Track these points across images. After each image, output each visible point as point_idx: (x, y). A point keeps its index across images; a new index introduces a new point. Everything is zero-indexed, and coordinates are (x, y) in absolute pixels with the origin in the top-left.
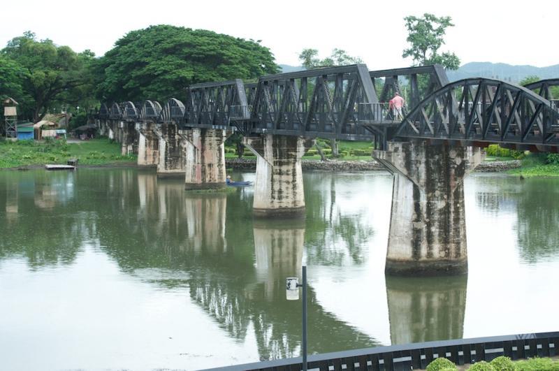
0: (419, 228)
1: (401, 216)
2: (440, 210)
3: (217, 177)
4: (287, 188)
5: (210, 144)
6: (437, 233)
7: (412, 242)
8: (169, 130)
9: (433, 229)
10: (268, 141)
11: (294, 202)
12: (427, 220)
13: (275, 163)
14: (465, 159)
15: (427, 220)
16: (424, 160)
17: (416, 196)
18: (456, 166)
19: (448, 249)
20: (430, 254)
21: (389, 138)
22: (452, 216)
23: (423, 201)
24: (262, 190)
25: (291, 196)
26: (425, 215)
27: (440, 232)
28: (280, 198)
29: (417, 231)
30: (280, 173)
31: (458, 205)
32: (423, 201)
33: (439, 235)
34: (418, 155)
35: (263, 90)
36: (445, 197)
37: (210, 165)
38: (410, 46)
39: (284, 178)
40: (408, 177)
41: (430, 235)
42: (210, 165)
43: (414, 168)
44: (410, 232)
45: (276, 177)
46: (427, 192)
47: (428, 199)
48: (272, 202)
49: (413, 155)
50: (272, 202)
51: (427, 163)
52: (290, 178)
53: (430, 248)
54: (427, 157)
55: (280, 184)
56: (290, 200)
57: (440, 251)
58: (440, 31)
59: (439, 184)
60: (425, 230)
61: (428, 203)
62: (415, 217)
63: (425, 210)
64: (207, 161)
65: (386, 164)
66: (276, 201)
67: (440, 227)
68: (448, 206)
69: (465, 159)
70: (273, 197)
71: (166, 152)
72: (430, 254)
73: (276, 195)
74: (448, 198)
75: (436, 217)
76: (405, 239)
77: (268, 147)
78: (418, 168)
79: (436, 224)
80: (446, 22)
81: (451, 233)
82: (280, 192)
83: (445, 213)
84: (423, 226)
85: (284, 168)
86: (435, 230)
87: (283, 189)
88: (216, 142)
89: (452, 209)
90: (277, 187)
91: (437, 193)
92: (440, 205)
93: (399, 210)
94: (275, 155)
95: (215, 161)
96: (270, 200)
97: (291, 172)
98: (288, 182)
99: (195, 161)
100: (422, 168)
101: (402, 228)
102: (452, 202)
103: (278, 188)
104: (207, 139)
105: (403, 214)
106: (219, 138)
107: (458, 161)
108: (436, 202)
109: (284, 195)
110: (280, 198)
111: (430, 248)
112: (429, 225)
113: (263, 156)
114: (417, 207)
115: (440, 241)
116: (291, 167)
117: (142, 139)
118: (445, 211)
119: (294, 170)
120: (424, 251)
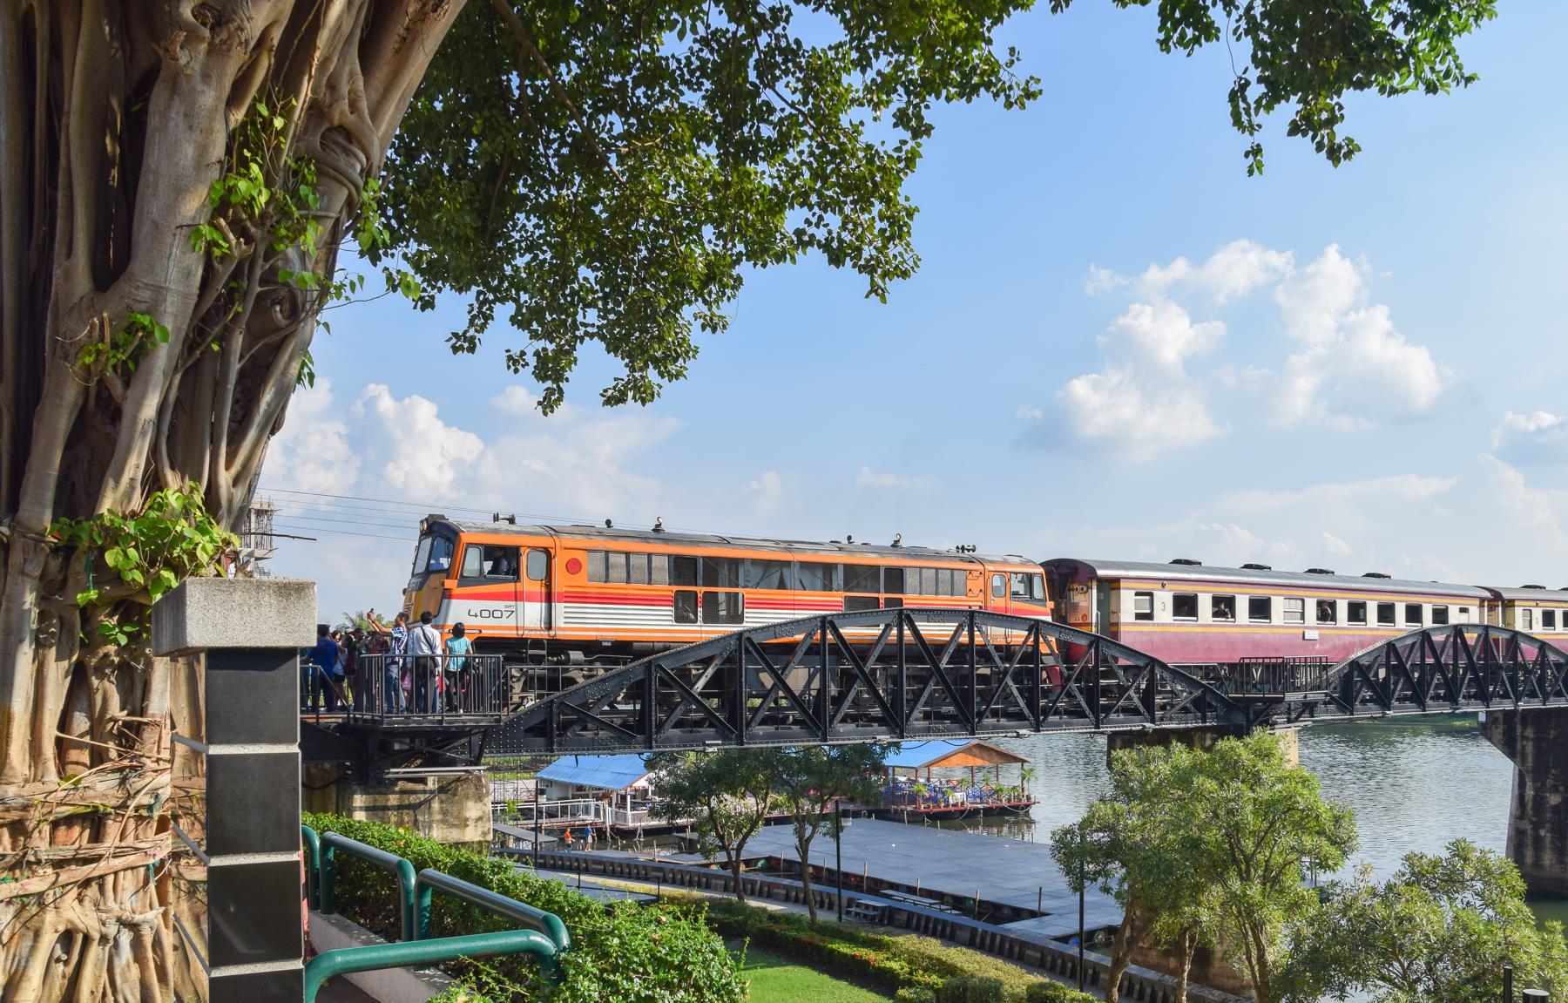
0: (1522, 828)
2: (1554, 807)
9: (1542, 833)
12: (1534, 819)
15: (1534, 819)
16: (1532, 736)
17: (1522, 785)
23: (1530, 793)
26: (1530, 812)
27: (1552, 838)
33: (1552, 842)
34: (1524, 728)
41: (1538, 841)
46: (1535, 781)
47: (1536, 790)
49: (1519, 730)
51: (1537, 741)
60: (1529, 832)
62: (1518, 812)
63: (1530, 804)
67: (1553, 831)
78: (1523, 747)
84: (1529, 827)
91: (1549, 782)
92: (1554, 800)
100: (1529, 748)
112: (1537, 826)
115: (1552, 850)
120: (1529, 859)
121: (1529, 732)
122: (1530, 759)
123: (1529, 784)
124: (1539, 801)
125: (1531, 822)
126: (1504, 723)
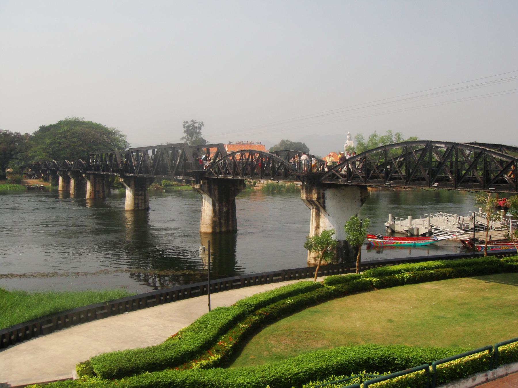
1: (207, 215)
4: (141, 202)
6: (224, 223)
7: (212, 227)
8: (77, 175)
9: (222, 221)
15: (219, 217)
16: (217, 188)
17: (214, 206)
21: (201, 179)
22: (231, 214)
23: (217, 207)
24: (129, 203)
25: (143, 206)
26: (218, 214)
30: (138, 195)
35: (131, 155)
37: (99, 191)
38: (185, 135)
39: (140, 197)
40: (210, 196)
42: (99, 191)
43: (213, 192)
44: (211, 223)
45: (136, 197)
46: (219, 204)
47: (219, 207)
49: (212, 186)
52: (143, 197)
55: (138, 200)
58: (200, 128)
59: (224, 200)
60: (218, 221)
63: (218, 211)
64: (97, 190)
65: (200, 191)
68: (228, 210)
70: (135, 206)
71: (74, 185)
76: (209, 226)
78: (214, 192)
79: (223, 218)
80: (202, 124)
81: (230, 222)
82: (138, 204)
85: (140, 193)
87: (140, 203)
89: (231, 211)
90: (136, 202)
91: (224, 204)
92: (225, 209)
93: (206, 212)
94: (135, 187)
95: (101, 189)
97: (143, 195)
98: (142, 199)
99: (91, 189)
100: (216, 192)
101: (207, 221)
102: (230, 208)
105: (208, 214)
107: (233, 189)
109: (140, 205)
112: (220, 219)
113: (130, 187)
114: (214, 210)
116: (143, 192)
117: (61, 179)
118: (227, 212)
119: (145, 194)
121: (216, 187)
122: (217, 196)
123: (217, 205)
124: (220, 210)
126: (208, 184)
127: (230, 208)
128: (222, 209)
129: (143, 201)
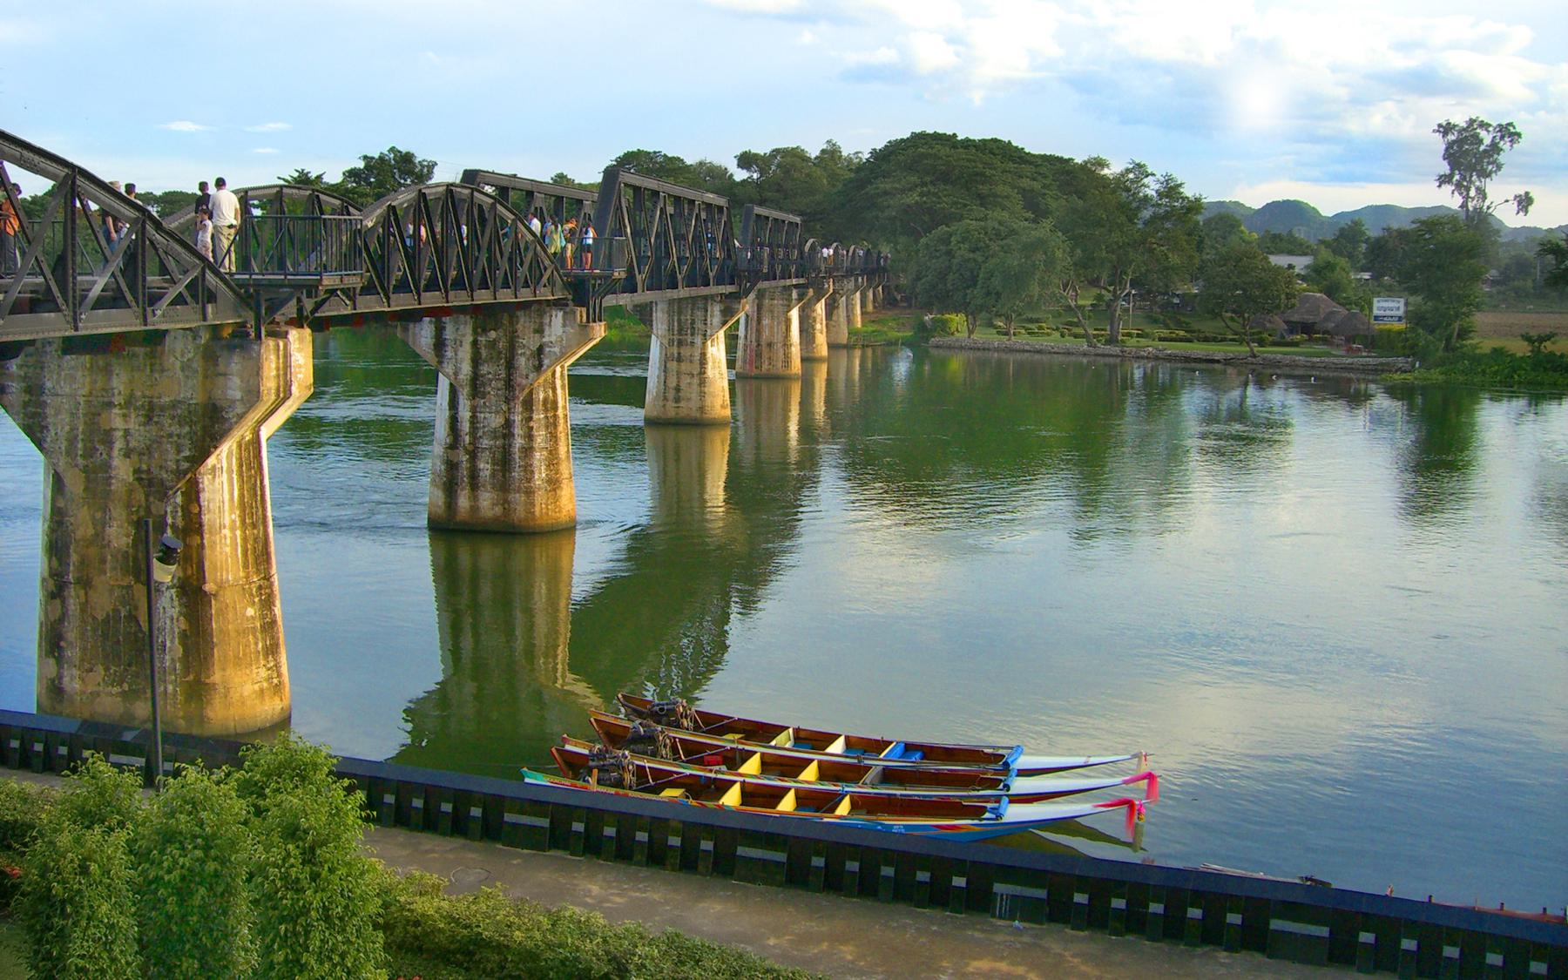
2: (495, 431)
3: (780, 364)
5: (772, 312)
7: (445, 483)
10: (659, 307)
11: (702, 409)
13: (671, 342)
14: (546, 340)
16: (470, 339)
18: (528, 353)
19: (509, 503)
20: (474, 509)
22: (519, 442)
23: (465, 414)
25: (694, 396)
26: (467, 439)
28: (677, 400)
29: (452, 466)
31: (532, 424)
32: (465, 414)
33: (493, 475)
36: (504, 407)
37: (770, 345)
39: (684, 367)
41: (474, 475)
43: (449, 353)
44: (443, 467)
45: (673, 365)
47: (474, 410)
48: (664, 406)
50: (664, 406)
53: (474, 498)
54: (475, 332)
55: (678, 378)
56: (694, 405)
57: (494, 505)
60: (465, 465)
61: (474, 420)
66: (671, 404)
69: (546, 340)
70: (665, 399)
72: (474, 509)
73: (671, 394)
74: (509, 409)
75: (485, 442)
77: (660, 314)
82: (678, 389)
83: (504, 436)
84: (464, 457)
85: (686, 351)
86: (485, 467)
88: (781, 308)
89: (518, 431)
90: (672, 382)
92: (496, 421)
94: (670, 329)
96: (661, 403)
97: (697, 357)
100: (465, 353)
103: (675, 384)
104: (766, 302)
106: (785, 302)
108: (488, 415)
110: (677, 400)
111: (474, 498)
119: (703, 355)
120: (463, 502)
125: (467, 452)
127: (517, 418)
128: (485, 418)
129: (696, 381)
